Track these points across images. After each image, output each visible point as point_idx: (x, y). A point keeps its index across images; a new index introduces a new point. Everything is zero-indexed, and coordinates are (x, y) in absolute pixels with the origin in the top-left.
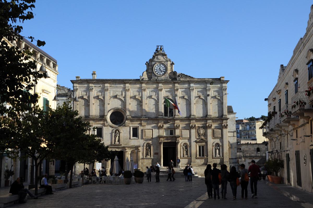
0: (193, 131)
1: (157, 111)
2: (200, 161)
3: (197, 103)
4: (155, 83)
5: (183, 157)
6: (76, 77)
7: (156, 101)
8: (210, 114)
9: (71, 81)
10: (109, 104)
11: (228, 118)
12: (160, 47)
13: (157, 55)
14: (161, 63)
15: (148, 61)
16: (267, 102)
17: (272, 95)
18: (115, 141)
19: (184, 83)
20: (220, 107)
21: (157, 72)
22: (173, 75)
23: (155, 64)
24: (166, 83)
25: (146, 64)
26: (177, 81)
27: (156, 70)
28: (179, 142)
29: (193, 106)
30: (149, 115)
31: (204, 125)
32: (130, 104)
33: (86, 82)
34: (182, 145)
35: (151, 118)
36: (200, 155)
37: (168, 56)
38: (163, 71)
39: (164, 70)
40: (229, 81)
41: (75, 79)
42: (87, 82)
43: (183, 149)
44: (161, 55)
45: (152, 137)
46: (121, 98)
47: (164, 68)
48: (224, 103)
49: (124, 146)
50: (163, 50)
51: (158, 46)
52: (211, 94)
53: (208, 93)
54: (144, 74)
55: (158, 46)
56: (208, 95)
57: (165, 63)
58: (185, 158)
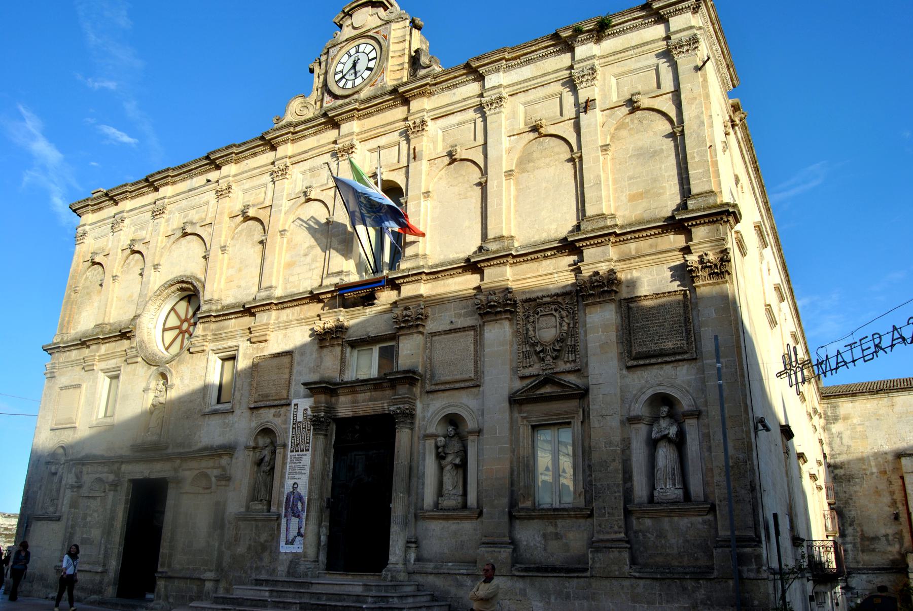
2: (544, 536)
3: (523, 171)
8: (599, 213)
10: (156, 267)
27: (338, 77)
29: (500, 185)
39: (372, 64)
43: (440, 457)
45: (284, 393)
48: (686, 123)
52: (605, 96)
56: (588, 106)
57: (377, 32)
58: (447, 518)
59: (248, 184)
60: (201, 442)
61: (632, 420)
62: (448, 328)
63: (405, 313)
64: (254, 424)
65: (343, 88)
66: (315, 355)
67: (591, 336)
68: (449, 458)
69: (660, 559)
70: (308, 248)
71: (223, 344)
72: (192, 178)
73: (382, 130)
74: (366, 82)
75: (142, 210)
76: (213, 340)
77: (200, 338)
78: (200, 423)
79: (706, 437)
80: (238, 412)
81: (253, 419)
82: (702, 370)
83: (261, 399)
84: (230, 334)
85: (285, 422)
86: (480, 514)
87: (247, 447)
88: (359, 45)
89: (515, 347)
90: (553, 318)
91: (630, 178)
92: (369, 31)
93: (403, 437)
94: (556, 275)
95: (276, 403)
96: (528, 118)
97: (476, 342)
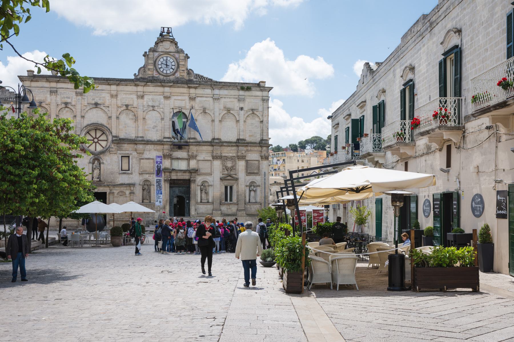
0: (217, 164)
1: (162, 130)
4: (158, 86)
5: (201, 202)
6: (28, 71)
7: (159, 115)
9: (18, 76)
10: (83, 117)
11: (270, 143)
12: (167, 29)
13: (162, 42)
14: (168, 53)
15: (147, 51)
16: (330, 121)
17: (341, 110)
18: (93, 178)
19: (204, 89)
23: (158, 57)
24: (176, 87)
25: (144, 56)
26: (195, 84)
27: (160, 66)
28: (195, 181)
31: (234, 155)
32: (118, 118)
34: (200, 184)
35: (152, 142)
36: (226, 200)
37: (179, 45)
38: (172, 68)
39: (173, 67)
40: (272, 88)
41: (26, 74)
43: (201, 191)
44: (169, 42)
45: (152, 171)
46: (104, 108)
47: (173, 64)
50: (171, 34)
51: (164, 28)
53: (242, 105)
54: (141, 72)
55: (164, 28)
56: (242, 109)
59: (124, 96)
61: (247, 186)
62: (203, 159)
64: (141, 178)
68: (204, 191)
69: (250, 213)
76: (119, 150)
79: (261, 191)
80: (134, 174)
82: (262, 177)
85: (153, 179)
86: (213, 204)
87: (139, 185)
89: (221, 167)
92: (171, 52)
93: (193, 186)
97: (211, 164)
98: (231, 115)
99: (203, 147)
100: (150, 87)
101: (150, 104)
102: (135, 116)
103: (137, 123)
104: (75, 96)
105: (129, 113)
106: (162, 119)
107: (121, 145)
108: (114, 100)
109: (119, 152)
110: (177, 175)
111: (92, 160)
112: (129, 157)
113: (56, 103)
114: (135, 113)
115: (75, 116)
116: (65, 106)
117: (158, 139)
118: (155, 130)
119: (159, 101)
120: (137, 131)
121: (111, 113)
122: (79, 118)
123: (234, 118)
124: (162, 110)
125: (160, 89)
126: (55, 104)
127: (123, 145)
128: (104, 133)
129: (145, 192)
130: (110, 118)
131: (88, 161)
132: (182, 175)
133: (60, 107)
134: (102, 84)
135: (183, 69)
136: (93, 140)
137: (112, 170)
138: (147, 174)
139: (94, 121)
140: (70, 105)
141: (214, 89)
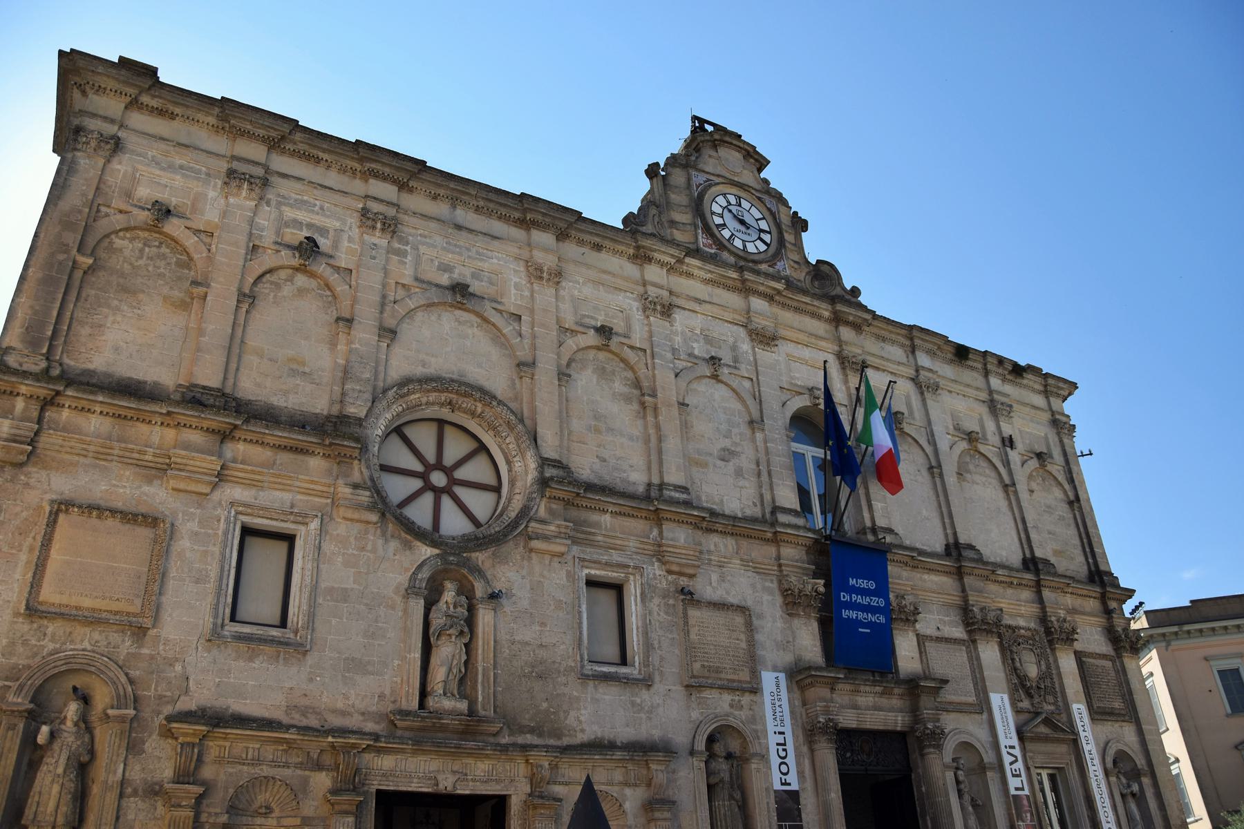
7: (738, 406)
10: (389, 333)
19: (884, 340)
20: (1069, 525)
21: (726, 233)
22: (809, 278)
24: (789, 307)
27: (718, 220)
30: (704, 498)
31: (1032, 625)
32: (563, 376)
33: (212, 120)
39: (767, 238)
40: (1074, 386)
42: (223, 118)
46: (495, 318)
47: (763, 225)
49: (520, 740)
53: (1007, 430)
59: (588, 291)
60: (583, 731)
63: (904, 602)
64: (695, 715)
65: (728, 240)
66: (779, 624)
67: (1065, 681)
70: (724, 450)
71: (602, 555)
72: (454, 207)
73: (806, 339)
74: (762, 256)
75: (315, 192)
76: (575, 541)
77: (552, 528)
78: (575, 694)
80: (659, 687)
81: (694, 705)
83: (707, 674)
84: (613, 541)
87: (692, 753)
88: (740, 198)
90: (1032, 653)
91: (1050, 533)
94: (1023, 608)
95: (735, 684)
96: (956, 423)
97: (970, 659)
98: (984, 464)
99: (926, 577)
100: (691, 282)
101: (699, 349)
102: (637, 384)
103: (650, 418)
104: (356, 231)
105: (609, 368)
106: (755, 424)
107: (584, 515)
108: (545, 294)
109: (576, 550)
110: (855, 707)
111: (425, 574)
112: (618, 589)
113: (251, 234)
114: (642, 371)
115: (349, 321)
116: (296, 262)
117: (748, 512)
118: (731, 467)
119: (734, 348)
120: (655, 451)
121: (534, 347)
122: (364, 335)
123: (993, 474)
124: (747, 384)
125: (734, 300)
126: (242, 239)
127: (595, 517)
128: (482, 448)
129: (724, 805)
130: (525, 366)
131: (403, 579)
132: (877, 708)
133: (267, 260)
134: (489, 214)
135: (796, 258)
136: (424, 476)
137: (542, 653)
138: (722, 688)
139: (443, 363)
140: (324, 260)
141: (913, 352)
